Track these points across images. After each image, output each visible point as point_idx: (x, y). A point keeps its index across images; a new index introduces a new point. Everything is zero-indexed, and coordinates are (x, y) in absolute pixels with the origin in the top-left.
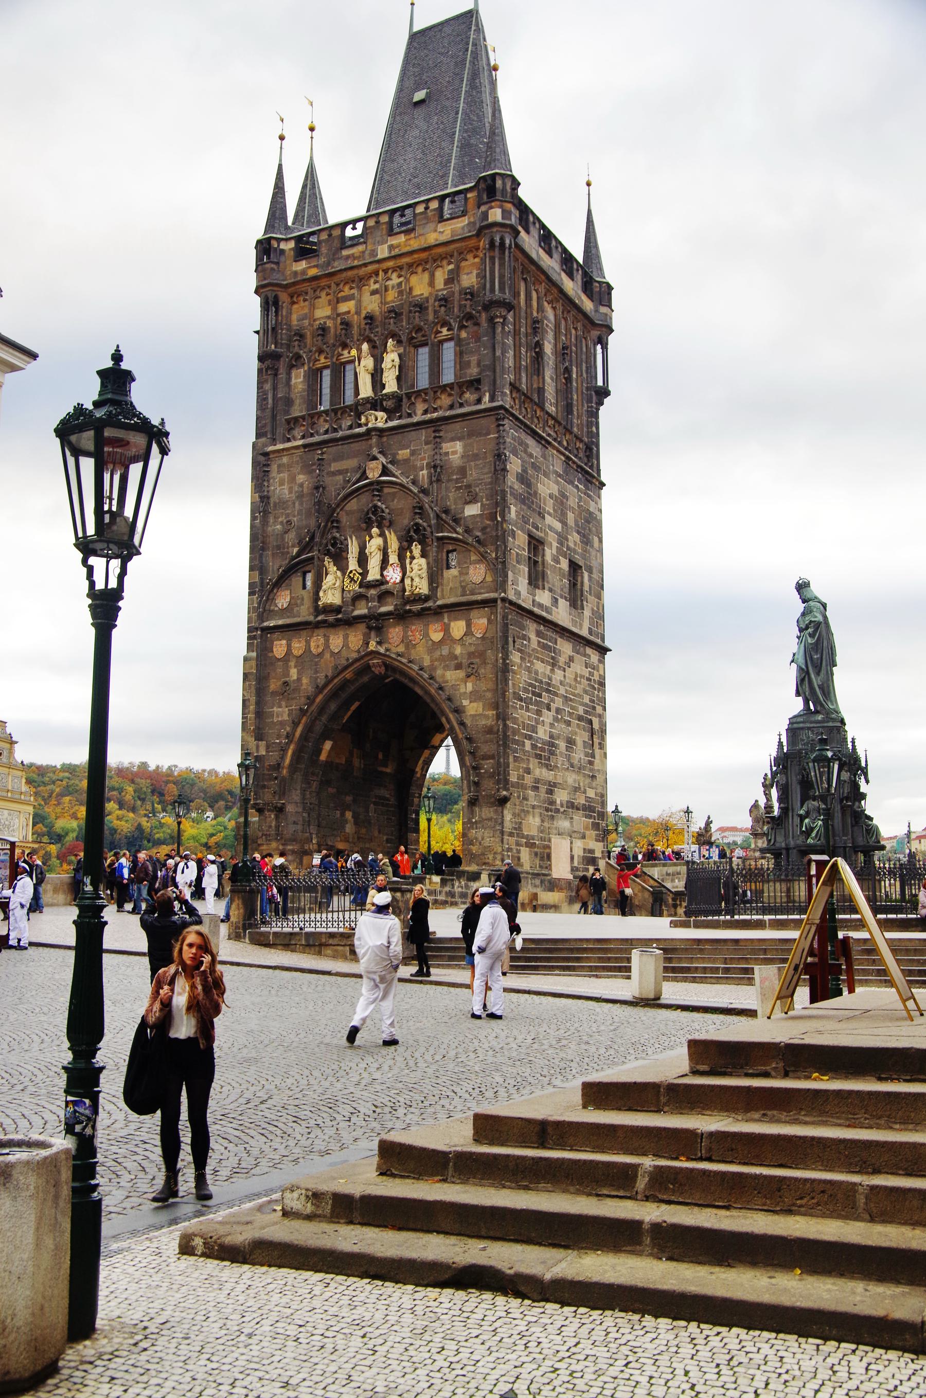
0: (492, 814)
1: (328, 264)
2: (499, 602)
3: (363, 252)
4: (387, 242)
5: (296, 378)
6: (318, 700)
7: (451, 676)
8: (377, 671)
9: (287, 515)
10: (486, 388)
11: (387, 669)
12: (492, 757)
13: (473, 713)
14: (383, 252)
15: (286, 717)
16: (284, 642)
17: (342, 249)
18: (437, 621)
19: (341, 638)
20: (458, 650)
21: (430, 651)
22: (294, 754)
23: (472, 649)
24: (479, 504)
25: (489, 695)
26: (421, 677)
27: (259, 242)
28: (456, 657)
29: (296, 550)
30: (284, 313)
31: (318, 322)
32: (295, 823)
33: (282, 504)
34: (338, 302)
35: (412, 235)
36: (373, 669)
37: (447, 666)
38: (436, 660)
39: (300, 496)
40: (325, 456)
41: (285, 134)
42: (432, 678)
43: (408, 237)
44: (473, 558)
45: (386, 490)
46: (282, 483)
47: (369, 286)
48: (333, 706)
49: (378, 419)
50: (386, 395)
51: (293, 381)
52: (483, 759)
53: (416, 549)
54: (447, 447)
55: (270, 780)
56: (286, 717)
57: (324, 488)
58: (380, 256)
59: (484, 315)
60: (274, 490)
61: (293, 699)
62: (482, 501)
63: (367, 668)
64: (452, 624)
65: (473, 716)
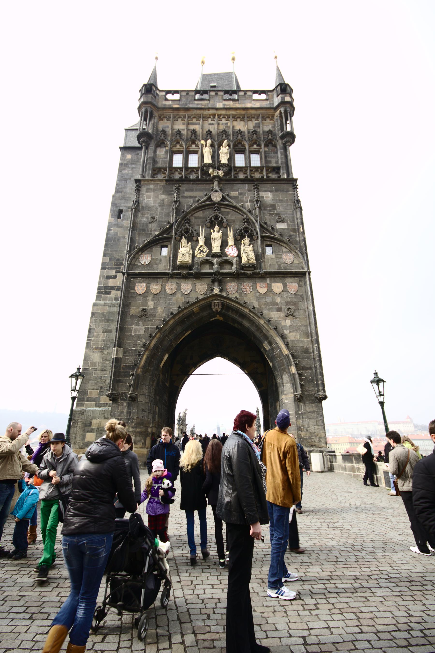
0: (314, 408)
1: (186, 105)
2: (307, 274)
3: (208, 104)
4: (222, 102)
5: (160, 152)
7: (275, 315)
8: (214, 309)
9: (153, 214)
10: (285, 171)
11: (222, 309)
12: (310, 368)
13: (292, 339)
14: (220, 105)
15: (142, 332)
16: (145, 284)
17: (195, 100)
18: (262, 282)
19: (190, 285)
20: (278, 300)
21: (258, 299)
22: (147, 358)
23: (289, 300)
24: (286, 224)
25: (303, 328)
26: (255, 314)
27: (145, 85)
28: (277, 304)
29: (157, 233)
30: (156, 121)
31: (175, 131)
32: (143, 410)
33: (149, 208)
34: (188, 124)
35: (237, 102)
36: (213, 307)
37: (271, 308)
38: (262, 304)
39: (162, 205)
40: (180, 188)
42: (262, 314)
43: (234, 102)
44: (284, 250)
45: (223, 210)
46: (149, 197)
47: (208, 121)
48: (179, 329)
49: (221, 173)
50: (224, 164)
52: (303, 370)
53: (246, 240)
54: (261, 194)
55: (125, 376)
56: (142, 332)
58: (217, 107)
59: (280, 141)
60: (142, 200)
61: (148, 321)
62: (287, 222)
64: (273, 284)
65: (293, 341)
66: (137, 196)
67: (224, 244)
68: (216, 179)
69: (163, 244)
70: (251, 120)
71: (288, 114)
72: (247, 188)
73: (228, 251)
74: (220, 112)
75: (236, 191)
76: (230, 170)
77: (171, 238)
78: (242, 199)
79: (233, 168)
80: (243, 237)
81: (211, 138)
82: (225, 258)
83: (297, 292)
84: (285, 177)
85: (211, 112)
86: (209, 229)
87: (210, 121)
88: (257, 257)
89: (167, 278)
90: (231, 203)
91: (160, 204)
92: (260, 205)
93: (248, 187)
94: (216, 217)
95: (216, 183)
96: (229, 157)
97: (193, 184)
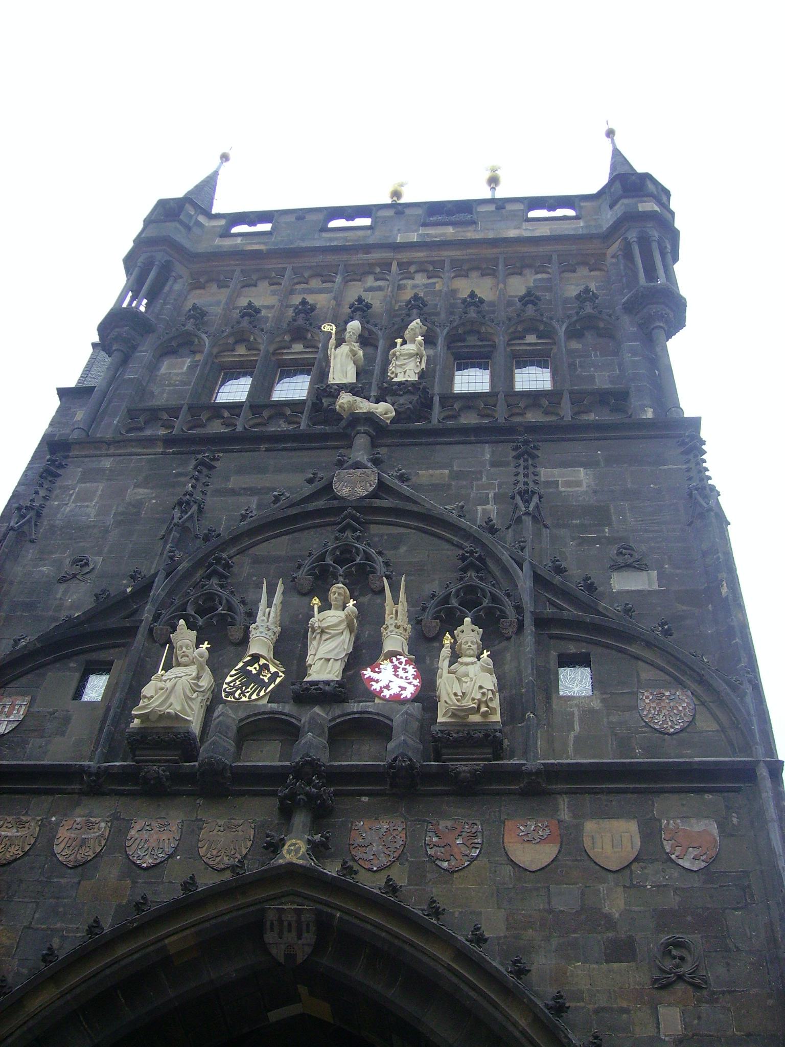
2: (763, 772)
6: (35, 1004)
7: (592, 982)
8: (278, 944)
11: (318, 947)
20: (615, 903)
23: (672, 901)
24: (654, 573)
28: (610, 923)
36: (270, 937)
41: (231, 157)
42: (521, 972)
43: (460, 229)
44: (647, 674)
45: (374, 529)
46: (84, 497)
51: (163, 370)
57: (200, 510)
59: (626, 319)
63: (253, 929)
64: (590, 826)
66: (42, 493)
67: (366, 652)
68: (362, 429)
69: (94, 656)
70: (520, 274)
71: (655, 246)
72: (488, 456)
73: (375, 676)
74: (405, 256)
75: (441, 468)
76: (427, 404)
77: (132, 631)
78: (463, 492)
79: (436, 399)
80: (451, 622)
81: (365, 321)
82: (355, 706)
83: (715, 860)
84: (649, 414)
85: (376, 256)
86: (306, 599)
87: (370, 281)
88: (513, 707)
89: (72, 793)
90: (415, 502)
91: (120, 518)
92: (537, 507)
93: (493, 452)
94: (344, 556)
95: (361, 441)
96: (423, 366)
97: (267, 450)
